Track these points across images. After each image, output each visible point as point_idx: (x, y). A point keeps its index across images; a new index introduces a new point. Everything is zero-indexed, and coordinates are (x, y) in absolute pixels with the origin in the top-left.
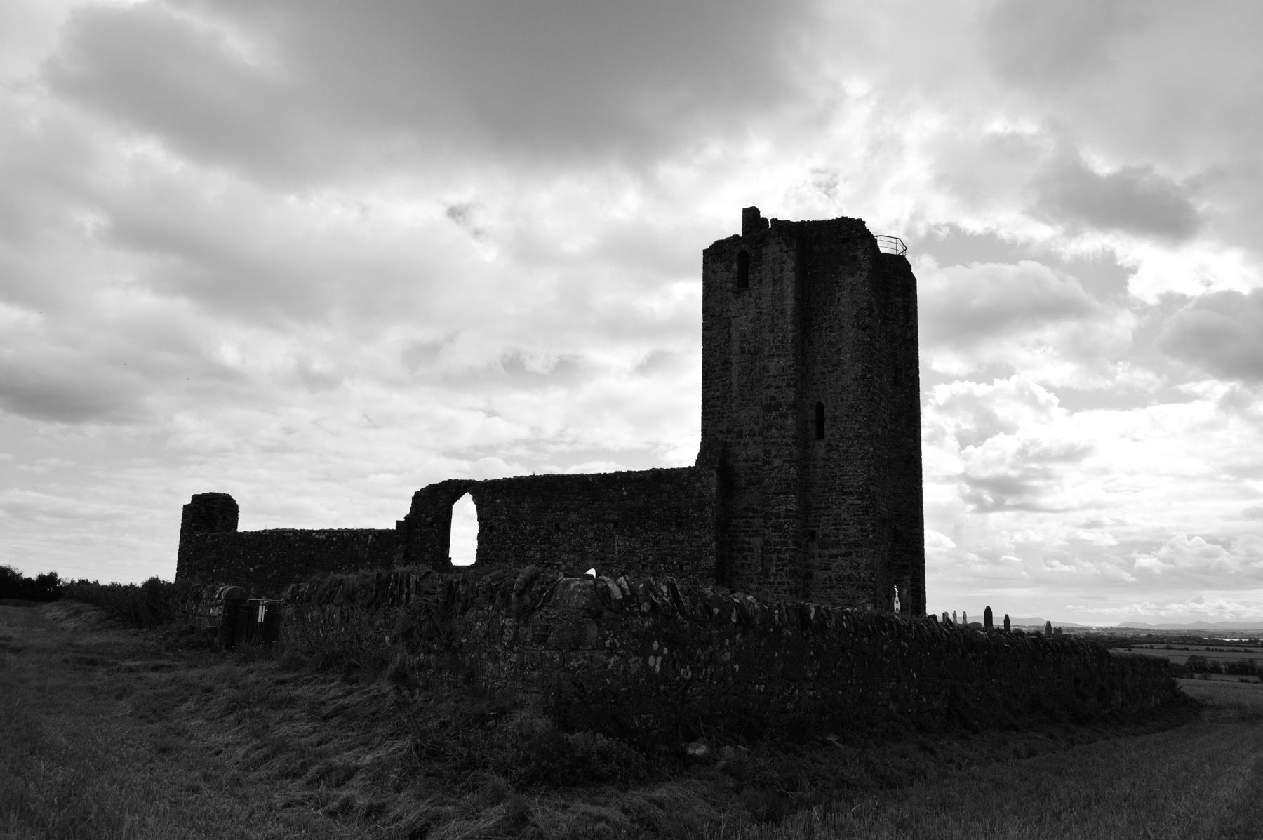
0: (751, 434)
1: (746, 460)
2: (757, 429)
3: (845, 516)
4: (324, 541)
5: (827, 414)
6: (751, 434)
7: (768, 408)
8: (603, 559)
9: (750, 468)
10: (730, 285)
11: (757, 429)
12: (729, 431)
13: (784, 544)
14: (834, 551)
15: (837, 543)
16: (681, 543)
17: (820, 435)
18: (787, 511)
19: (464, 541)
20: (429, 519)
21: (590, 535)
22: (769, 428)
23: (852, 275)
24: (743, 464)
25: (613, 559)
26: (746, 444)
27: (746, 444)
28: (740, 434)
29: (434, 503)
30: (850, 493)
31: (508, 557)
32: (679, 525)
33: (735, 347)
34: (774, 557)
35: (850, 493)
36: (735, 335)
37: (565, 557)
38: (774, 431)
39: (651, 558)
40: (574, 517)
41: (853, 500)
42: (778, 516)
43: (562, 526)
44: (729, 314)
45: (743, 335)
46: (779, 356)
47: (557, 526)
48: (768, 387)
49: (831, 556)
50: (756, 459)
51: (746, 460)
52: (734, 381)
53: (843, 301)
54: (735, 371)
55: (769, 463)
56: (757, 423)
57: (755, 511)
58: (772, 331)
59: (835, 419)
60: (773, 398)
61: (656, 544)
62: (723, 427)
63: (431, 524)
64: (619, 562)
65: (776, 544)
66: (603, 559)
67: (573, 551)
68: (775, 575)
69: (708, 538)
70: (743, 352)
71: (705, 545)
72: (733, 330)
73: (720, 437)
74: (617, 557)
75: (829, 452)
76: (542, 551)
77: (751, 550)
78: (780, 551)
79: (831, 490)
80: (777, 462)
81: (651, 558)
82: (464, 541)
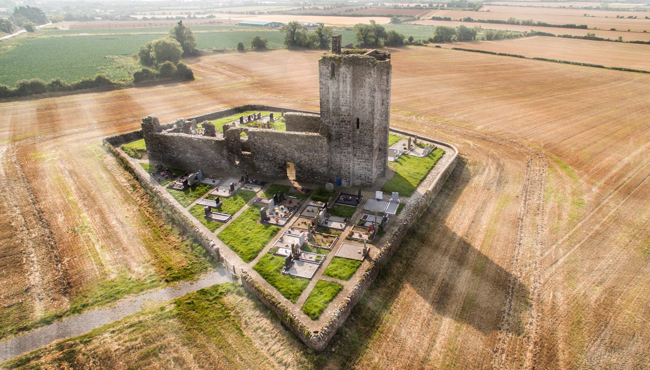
0: (336, 124)
5: (360, 122)
6: (336, 124)
10: (329, 75)
12: (330, 122)
17: (358, 127)
28: (333, 124)
33: (331, 96)
36: (330, 93)
41: (367, 147)
45: (333, 93)
62: (328, 121)
70: (333, 98)
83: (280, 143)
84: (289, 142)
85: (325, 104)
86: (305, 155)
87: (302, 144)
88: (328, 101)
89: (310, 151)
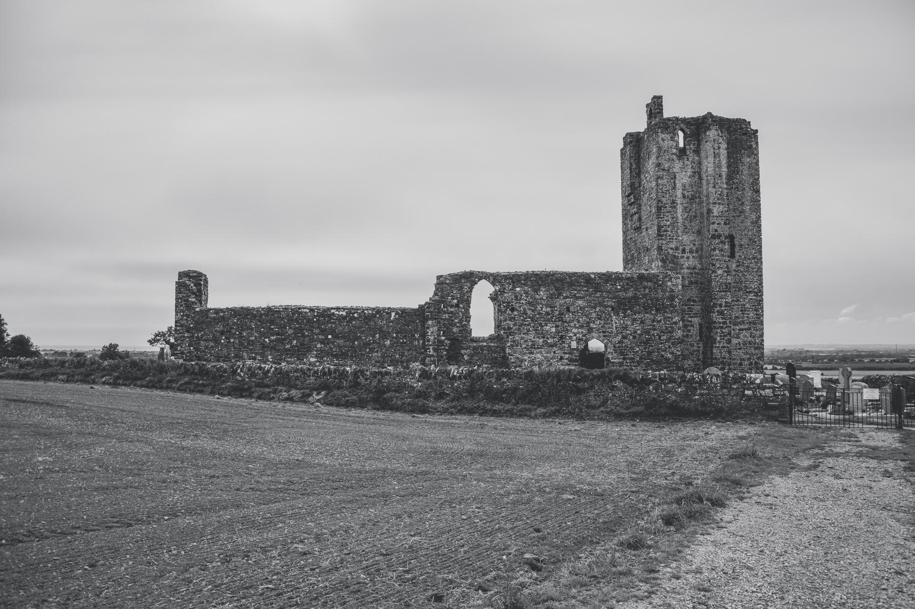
0: (691, 252)
1: (688, 268)
2: (694, 248)
3: (748, 306)
4: (344, 318)
6: (691, 252)
7: (714, 237)
8: (604, 332)
9: (691, 273)
11: (694, 248)
12: (677, 249)
13: (724, 323)
14: (742, 327)
15: (743, 322)
16: (660, 321)
17: (732, 255)
18: (726, 302)
19: (482, 320)
20: (455, 301)
21: (594, 315)
22: (714, 250)
23: (749, 157)
24: (686, 271)
25: (612, 332)
26: (688, 258)
27: (688, 258)
28: (684, 251)
29: (455, 288)
30: (750, 292)
31: (529, 330)
32: (657, 310)
33: (679, 193)
34: (719, 331)
35: (750, 292)
36: (679, 185)
37: (575, 330)
38: (717, 252)
39: (639, 332)
40: (580, 302)
42: (721, 305)
43: (572, 309)
44: (675, 170)
45: (684, 186)
46: (719, 204)
47: (568, 310)
48: (713, 223)
49: (742, 330)
50: (694, 268)
51: (688, 268)
52: (679, 215)
53: (745, 173)
54: (680, 209)
55: (715, 272)
56: (694, 245)
57: (694, 301)
58: (714, 187)
59: (741, 246)
60: (716, 231)
61: (642, 322)
62: (673, 246)
63: (457, 306)
64: (617, 335)
65: (720, 323)
66: (604, 332)
67: (582, 327)
68: (720, 342)
69: (676, 319)
70: (684, 197)
71: (676, 323)
72: (677, 182)
73: (671, 252)
74: (614, 330)
75: (738, 266)
76: (557, 326)
77: (692, 326)
78: (722, 328)
79: (740, 289)
80: (720, 272)
81: (639, 332)
82: (482, 320)
83: (577, 298)
84: (598, 294)
85: (669, 209)
86: (634, 320)
87: (630, 294)
88: (673, 202)
89: (647, 309)
